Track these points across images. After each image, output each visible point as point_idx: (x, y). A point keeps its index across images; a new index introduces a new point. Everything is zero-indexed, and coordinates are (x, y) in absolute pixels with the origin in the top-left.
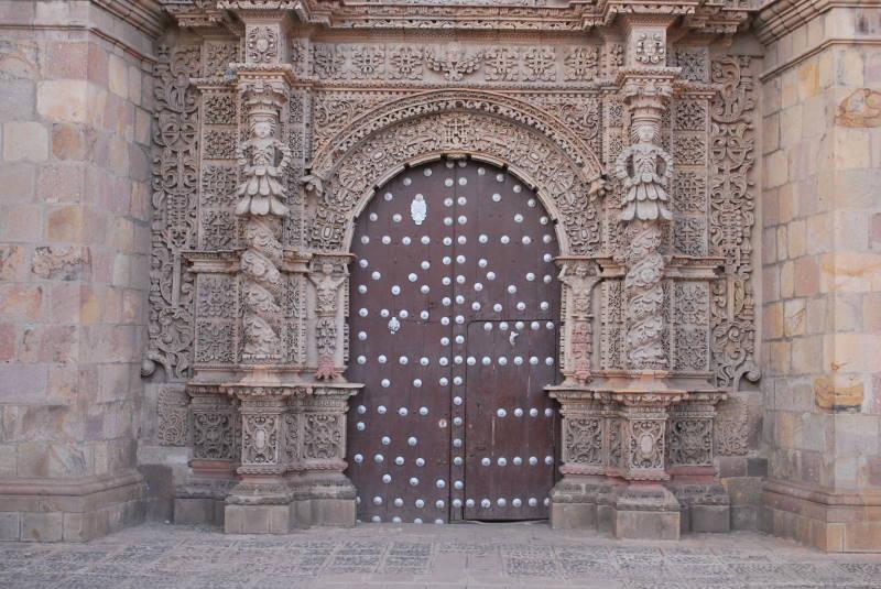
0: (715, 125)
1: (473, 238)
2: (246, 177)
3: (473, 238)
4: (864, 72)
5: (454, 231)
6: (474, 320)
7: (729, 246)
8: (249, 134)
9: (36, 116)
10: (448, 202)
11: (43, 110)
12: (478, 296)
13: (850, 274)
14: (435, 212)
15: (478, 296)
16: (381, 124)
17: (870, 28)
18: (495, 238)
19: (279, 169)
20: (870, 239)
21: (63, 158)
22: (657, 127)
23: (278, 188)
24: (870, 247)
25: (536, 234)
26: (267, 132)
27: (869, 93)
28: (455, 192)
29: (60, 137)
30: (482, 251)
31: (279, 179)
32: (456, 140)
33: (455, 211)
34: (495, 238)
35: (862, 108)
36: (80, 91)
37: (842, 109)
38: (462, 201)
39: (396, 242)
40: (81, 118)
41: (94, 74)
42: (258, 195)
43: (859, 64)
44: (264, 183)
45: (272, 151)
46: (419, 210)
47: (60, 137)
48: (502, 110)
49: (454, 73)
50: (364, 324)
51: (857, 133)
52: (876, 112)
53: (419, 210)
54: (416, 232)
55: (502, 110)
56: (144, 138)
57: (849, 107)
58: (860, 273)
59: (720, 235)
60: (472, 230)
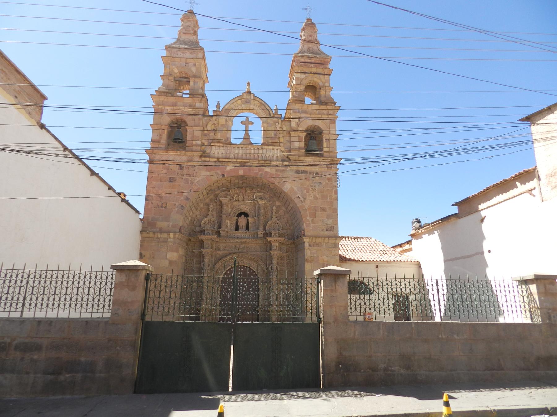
1: (243, 280)
3: (243, 280)
6: (244, 295)
8: (203, 261)
9: (166, 259)
11: (168, 257)
12: (244, 291)
15: (244, 291)
25: (255, 279)
27: (311, 257)
28: (241, 271)
29: (171, 262)
30: (245, 282)
36: (175, 254)
41: (177, 251)
50: (223, 296)
51: (309, 263)
56: (184, 261)
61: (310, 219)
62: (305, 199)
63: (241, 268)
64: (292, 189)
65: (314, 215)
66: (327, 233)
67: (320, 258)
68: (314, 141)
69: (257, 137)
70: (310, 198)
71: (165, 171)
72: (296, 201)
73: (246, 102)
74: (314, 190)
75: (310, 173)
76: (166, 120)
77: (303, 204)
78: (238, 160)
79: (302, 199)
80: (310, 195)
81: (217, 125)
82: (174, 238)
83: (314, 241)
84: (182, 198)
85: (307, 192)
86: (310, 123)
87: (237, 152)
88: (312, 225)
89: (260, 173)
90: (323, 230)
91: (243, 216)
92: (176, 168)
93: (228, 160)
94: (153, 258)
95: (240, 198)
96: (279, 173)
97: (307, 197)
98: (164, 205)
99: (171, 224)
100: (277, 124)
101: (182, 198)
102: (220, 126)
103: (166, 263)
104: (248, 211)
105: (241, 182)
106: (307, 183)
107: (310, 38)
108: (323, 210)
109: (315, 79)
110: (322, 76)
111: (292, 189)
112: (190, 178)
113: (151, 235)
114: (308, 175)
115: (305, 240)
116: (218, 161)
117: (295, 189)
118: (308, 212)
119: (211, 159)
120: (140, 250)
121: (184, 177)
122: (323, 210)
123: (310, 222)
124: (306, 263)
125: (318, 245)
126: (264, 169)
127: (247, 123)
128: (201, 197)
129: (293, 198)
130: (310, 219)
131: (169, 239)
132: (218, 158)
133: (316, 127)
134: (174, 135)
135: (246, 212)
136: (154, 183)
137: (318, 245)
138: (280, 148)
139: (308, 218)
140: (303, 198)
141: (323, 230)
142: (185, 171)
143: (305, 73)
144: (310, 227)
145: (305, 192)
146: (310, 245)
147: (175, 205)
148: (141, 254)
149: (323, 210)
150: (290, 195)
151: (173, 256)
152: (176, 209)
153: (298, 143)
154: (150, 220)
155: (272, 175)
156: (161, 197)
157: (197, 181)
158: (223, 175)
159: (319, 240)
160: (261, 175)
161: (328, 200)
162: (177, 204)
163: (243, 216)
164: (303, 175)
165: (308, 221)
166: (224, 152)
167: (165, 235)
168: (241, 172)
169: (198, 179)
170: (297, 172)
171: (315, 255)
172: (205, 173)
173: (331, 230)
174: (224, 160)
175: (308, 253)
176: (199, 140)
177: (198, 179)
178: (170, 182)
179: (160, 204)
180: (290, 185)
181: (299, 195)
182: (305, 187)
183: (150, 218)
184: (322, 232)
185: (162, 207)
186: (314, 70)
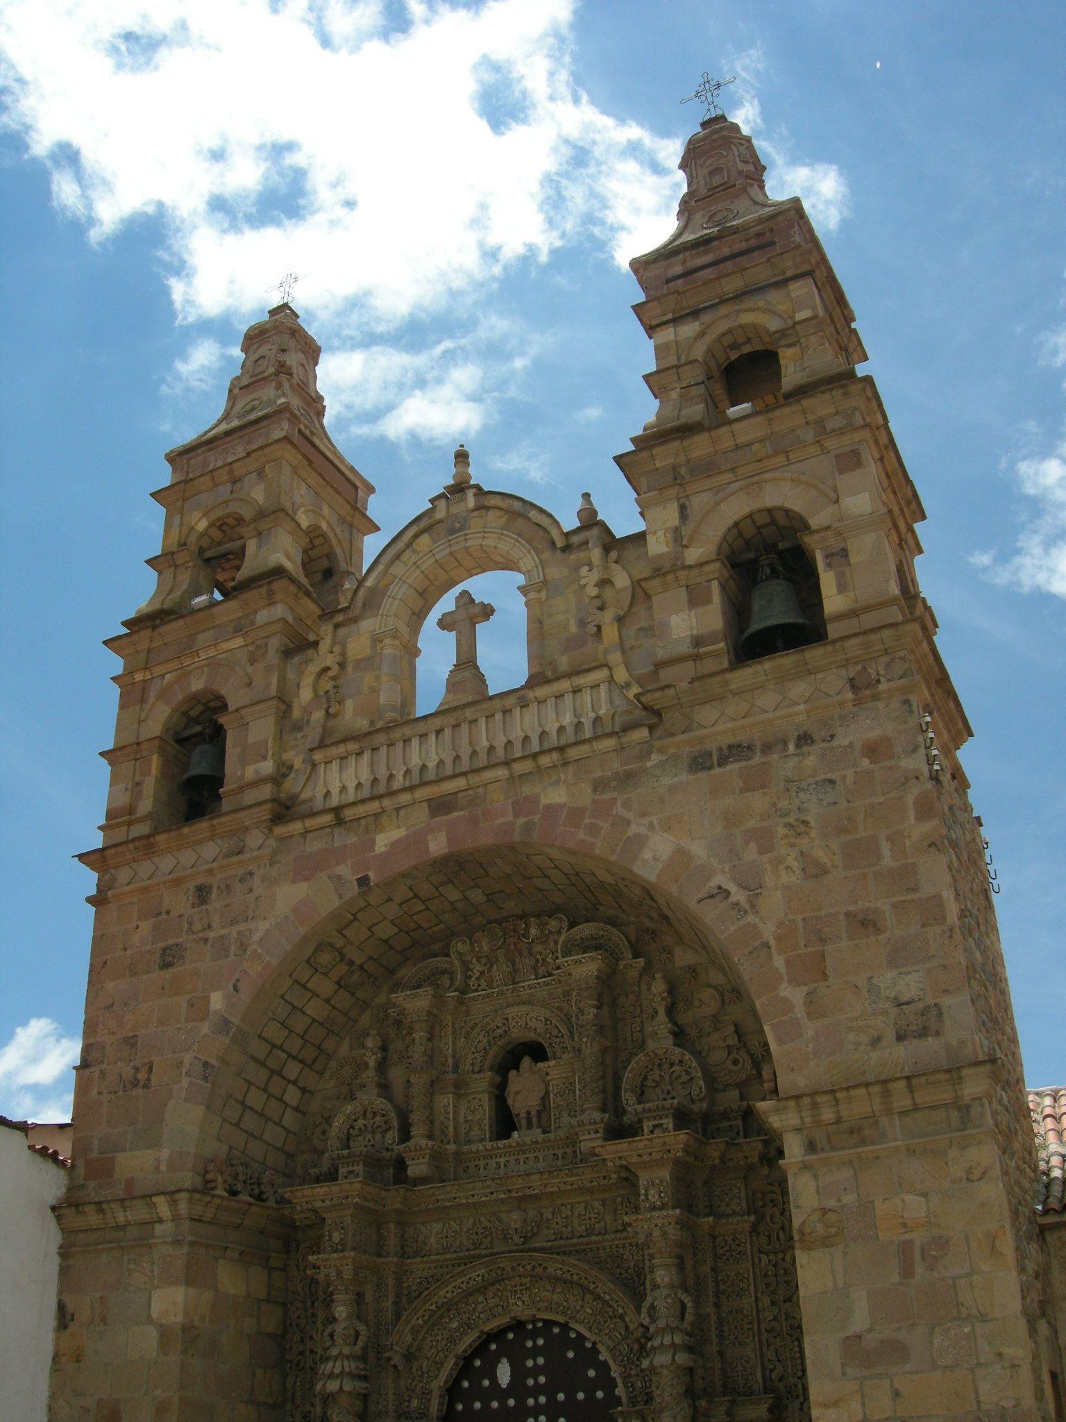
0: (763, 1257)
2: (325, 1359)
4: (818, 1192)
5: (536, 1391)
7: (792, 1380)
9: (150, 1320)
10: (530, 1363)
11: (155, 1314)
13: (826, 1406)
14: (519, 1373)
16: (449, 1295)
17: (819, 1146)
18: (571, 1396)
19: (357, 1348)
20: (843, 1366)
21: (166, 1354)
22: (673, 1270)
23: (351, 1366)
24: (844, 1374)
26: (344, 1315)
27: (825, 1211)
31: (355, 1358)
32: (519, 1303)
33: (536, 1371)
34: (571, 1396)
35: (820, 1228)
37: (801, 1233)
38: (541, 1361)
39: (486, 1406)
40: (179, 1319)
42: (331, 1376)
43: (812, 1184)
44: (338, 1364)
45: (352, 1331)
46: (504, 1374)
47: (165, 1333)
48: (551, 1270)
49: (517, 1239)
52: (834, 1230)
53: (504, 1374)
54: (502, 1395)
55: (551, 1270)
57: (807, 1229)
58: (835, 1404)
59: (779, 1369)
60: (550, 1390)
61: (795, 995)
62: (754, 889)
63: (534, 1335)
64: (681, 854)
65: (814, 969)
66: (901, 1055)
67: (881, 1208)
68: (775, 591)
69: (505, 660)
70: (785, 878)
71: (146, 926)
72: (710, 915)
73: (452, 531)
74: (800, 828)
75: (767, 748)
76: (158, 718)
77: (751, 918)
78: (422, 793)
79: (738, 895)
80: (778, 861)
81: (335, 670)
82: (176, 1218)
83: (827, 1115)
84: (205, 1028)
85: (762, 851)
86: (735, 509)
87: (415, 761)
88: (809, 1029)
89: (521, 821)
90: (876, 1042)
91: (526, 1062)
92: (180, 903)
93: (374, 806)
94: (104, 1320)
95: (499, 973)
96: (607, 796)
97: (769, 880)
98: (142, 1076)
99: (165, 1153)
100: (585, 569)
101: (205, 1028)
102: (350, 668)
103: (146, 1342)
104: (540, 1026)
105: (477, 896)
106: (759, 801)
107: (717, 180)
108: (867, 923)
109: (747, 318)
110: (774, 297)
111: (681, 854)
112: (234, 931)
113: (93, 1219)
114: (758, 759)
115: (775, 1121)
116: (340, 822)
117: (698, 850)
118: (779, 962)
119: (311, 823)
120: (60, 1292)
121: (211, 935)
122: (864, 924)
123: (800, 1011)
124: (801, 1257)
125: (858, 1133)
126: (536, 800)
127: (474, 614)
128: (315, 1009)
129: (692, 904)
130: (795, 995)
131: (159, 1228)
132: (337, 811)
133: (763, 519)
134: (184, 772)
135: (531, 1036)
136: (110, 985)
137: (858, 1133)
138: (603, 674)
139: (785, 991)
140: (743, 886)
141: (876, 1042)
142: (215, 904)
143: (695, 314)
144: (810, 1042)
145: (751, 854)
146: (811, 1147)
147: (180, 1064)
148: (61, 1307)
149: (867, 923)
150: (674, 890)
151: (171, 1302)
152: (185, 1081)
153: (690, 621)
154: (95, 1154)
155: (576, 815)
156: (131, 1041)
157: (256, 937)
158: (363, 881)
159: (859, 1105)
160: (528, 828)
161: (888, 861)
162: (188, 1058)
163: (526, 1062)
164: (732, 768)
165: (787, 1005)
166: (365, 776)
167: (138, 1213)
168: (437, 845)
169: (263, 926)
170: (700, 763)
171: (849, 1199)
172: (289, 895)
173: (923, 1033)
174: (361, 810)
175: (805, 1195)
176: (264, 758)
177: (262, 927)
178: (166, 965)
179: (128, 1072)
180: (670, 839)
181: (721, 879)
182: (752, 823)
183: (96, 1142)
184: (875, 1055)
185: (135, 1084)
186: (733, 284)
